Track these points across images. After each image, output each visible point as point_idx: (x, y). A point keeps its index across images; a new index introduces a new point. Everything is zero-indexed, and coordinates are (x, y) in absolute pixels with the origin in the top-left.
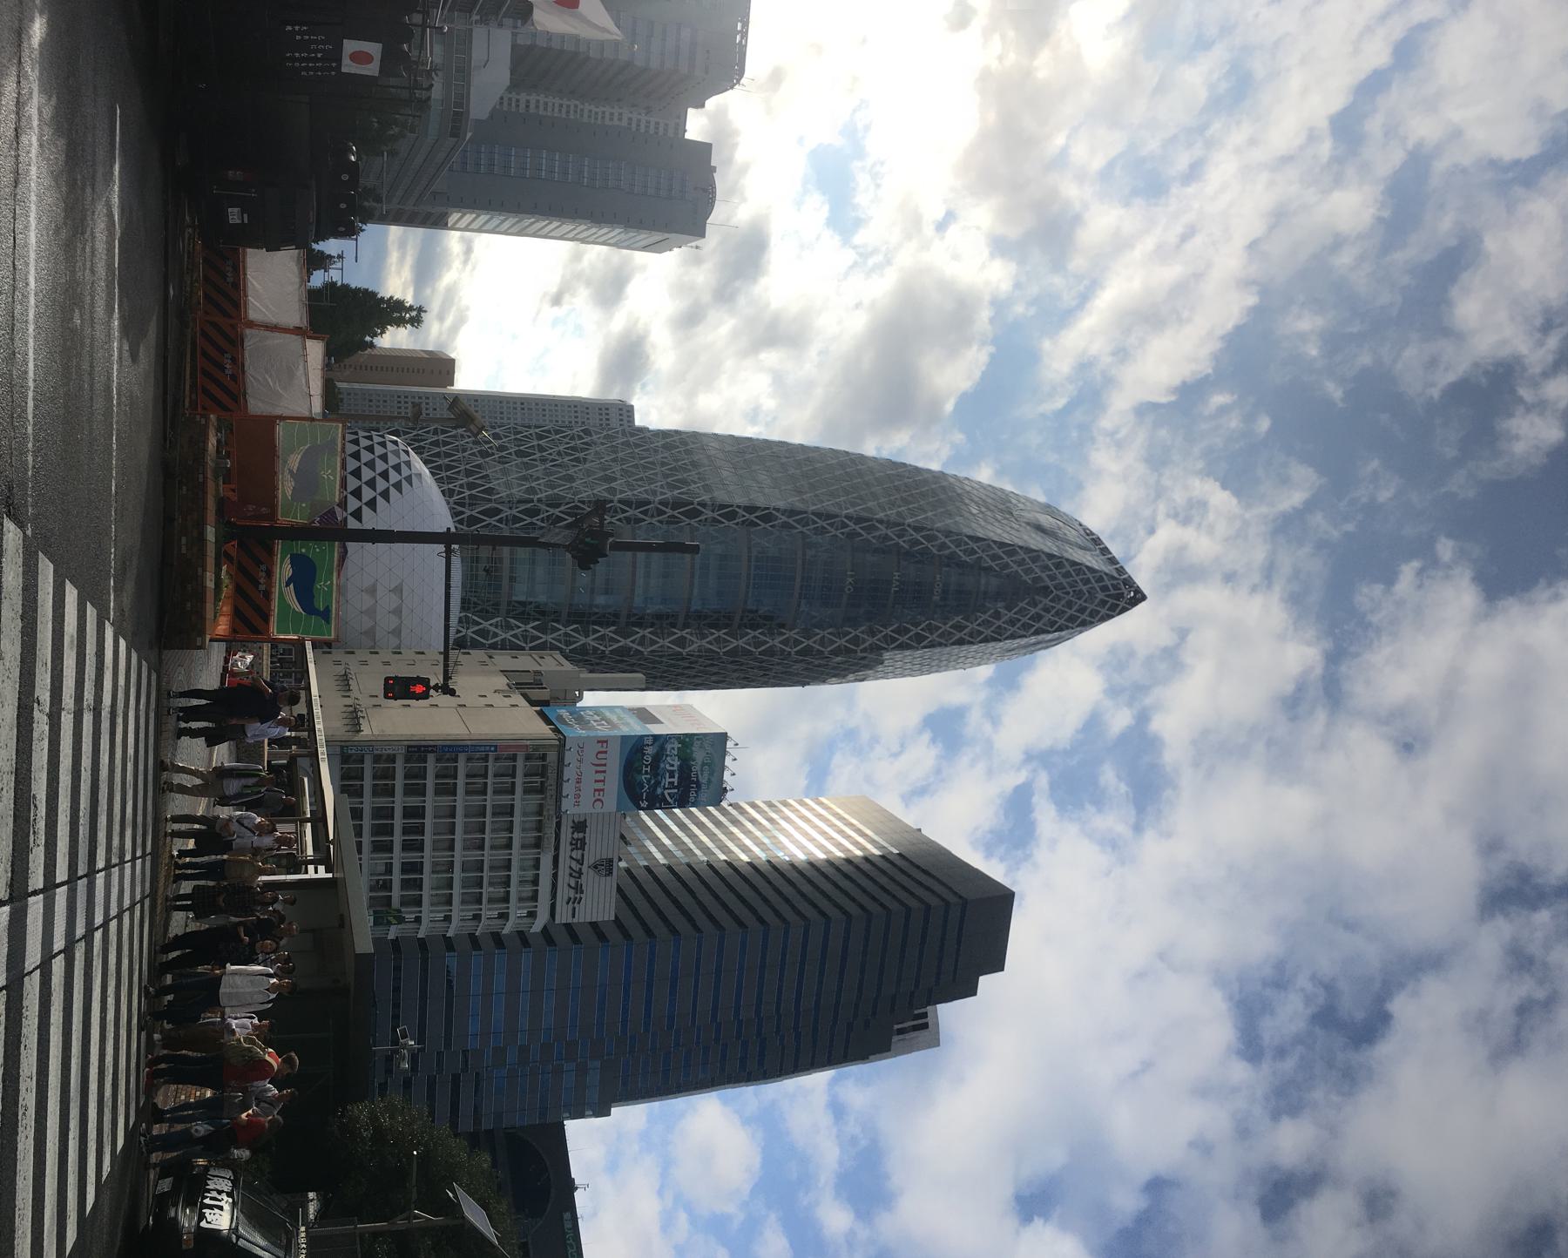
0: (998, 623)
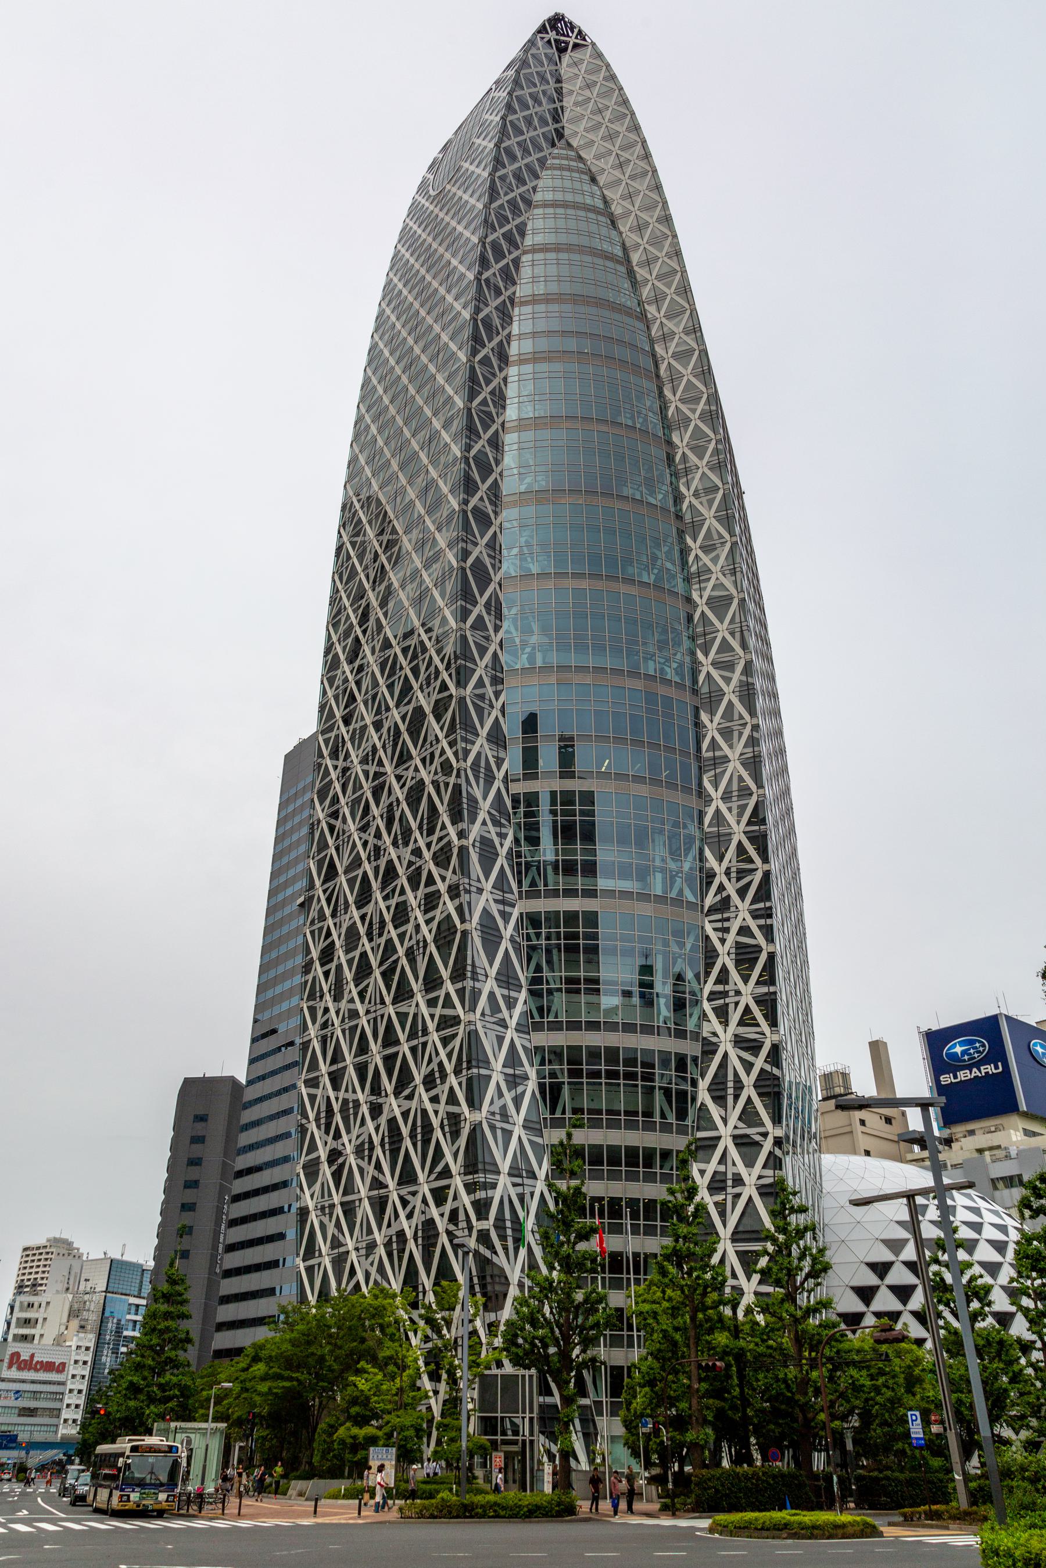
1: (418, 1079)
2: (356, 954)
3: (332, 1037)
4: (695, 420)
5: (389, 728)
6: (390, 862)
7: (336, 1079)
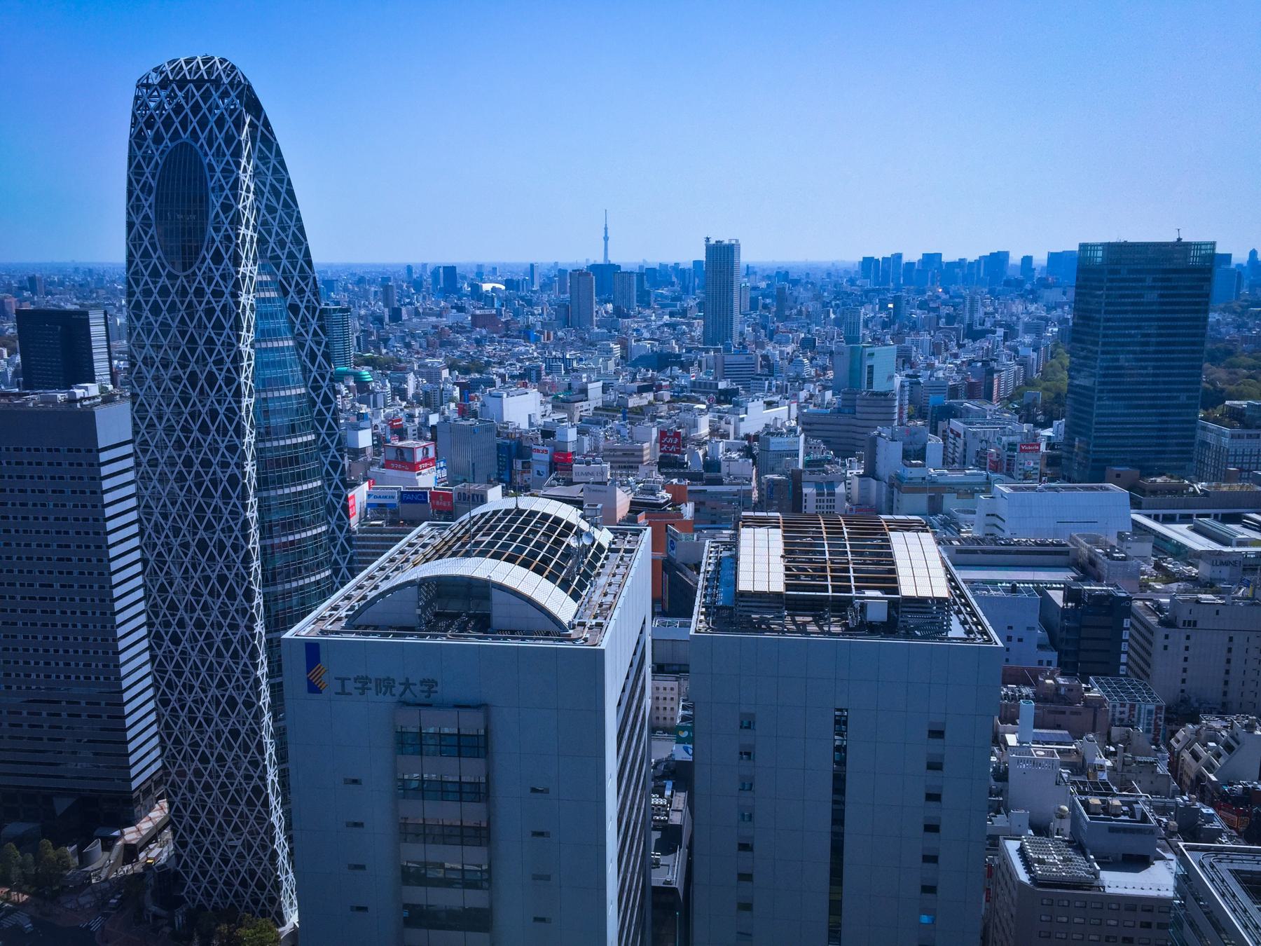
0: (303, 310)
1: (245, 831)
4: (339, 510)
6: (220, 754)
7: (196, 820)
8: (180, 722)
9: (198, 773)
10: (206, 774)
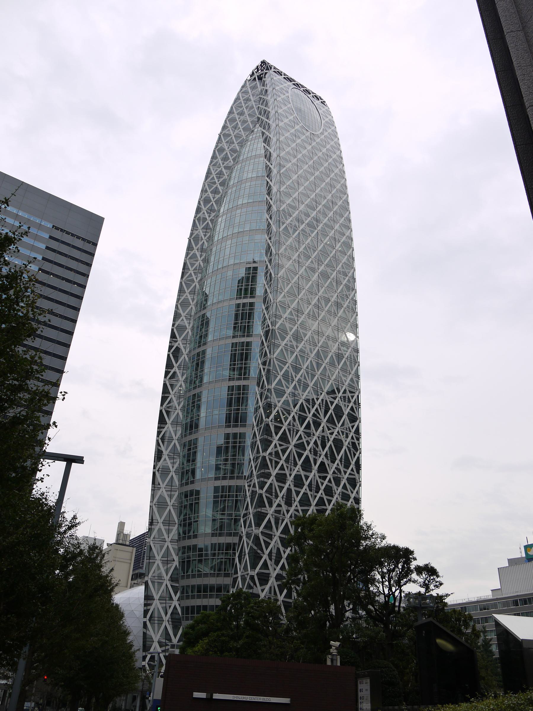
2: (303, 491)
3: (283, 520)
5: (322, 400)
8: (290, 418)
9: (298, 481)
10: (307, 483)
